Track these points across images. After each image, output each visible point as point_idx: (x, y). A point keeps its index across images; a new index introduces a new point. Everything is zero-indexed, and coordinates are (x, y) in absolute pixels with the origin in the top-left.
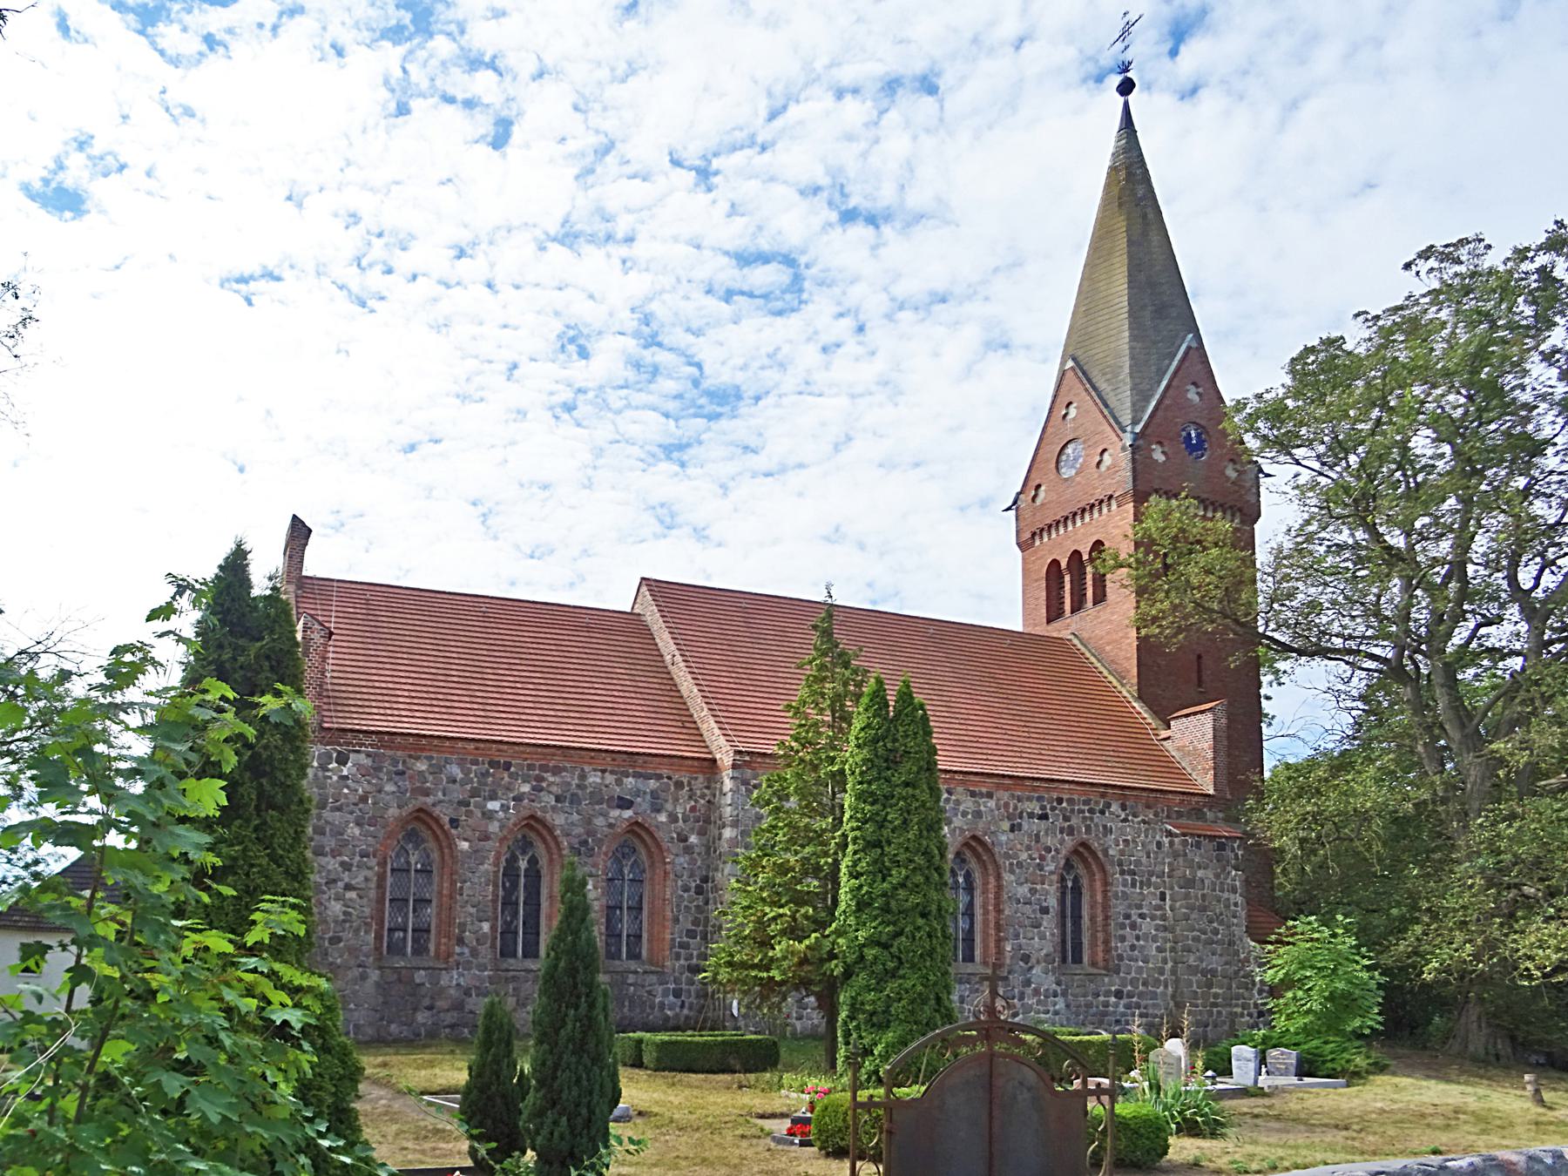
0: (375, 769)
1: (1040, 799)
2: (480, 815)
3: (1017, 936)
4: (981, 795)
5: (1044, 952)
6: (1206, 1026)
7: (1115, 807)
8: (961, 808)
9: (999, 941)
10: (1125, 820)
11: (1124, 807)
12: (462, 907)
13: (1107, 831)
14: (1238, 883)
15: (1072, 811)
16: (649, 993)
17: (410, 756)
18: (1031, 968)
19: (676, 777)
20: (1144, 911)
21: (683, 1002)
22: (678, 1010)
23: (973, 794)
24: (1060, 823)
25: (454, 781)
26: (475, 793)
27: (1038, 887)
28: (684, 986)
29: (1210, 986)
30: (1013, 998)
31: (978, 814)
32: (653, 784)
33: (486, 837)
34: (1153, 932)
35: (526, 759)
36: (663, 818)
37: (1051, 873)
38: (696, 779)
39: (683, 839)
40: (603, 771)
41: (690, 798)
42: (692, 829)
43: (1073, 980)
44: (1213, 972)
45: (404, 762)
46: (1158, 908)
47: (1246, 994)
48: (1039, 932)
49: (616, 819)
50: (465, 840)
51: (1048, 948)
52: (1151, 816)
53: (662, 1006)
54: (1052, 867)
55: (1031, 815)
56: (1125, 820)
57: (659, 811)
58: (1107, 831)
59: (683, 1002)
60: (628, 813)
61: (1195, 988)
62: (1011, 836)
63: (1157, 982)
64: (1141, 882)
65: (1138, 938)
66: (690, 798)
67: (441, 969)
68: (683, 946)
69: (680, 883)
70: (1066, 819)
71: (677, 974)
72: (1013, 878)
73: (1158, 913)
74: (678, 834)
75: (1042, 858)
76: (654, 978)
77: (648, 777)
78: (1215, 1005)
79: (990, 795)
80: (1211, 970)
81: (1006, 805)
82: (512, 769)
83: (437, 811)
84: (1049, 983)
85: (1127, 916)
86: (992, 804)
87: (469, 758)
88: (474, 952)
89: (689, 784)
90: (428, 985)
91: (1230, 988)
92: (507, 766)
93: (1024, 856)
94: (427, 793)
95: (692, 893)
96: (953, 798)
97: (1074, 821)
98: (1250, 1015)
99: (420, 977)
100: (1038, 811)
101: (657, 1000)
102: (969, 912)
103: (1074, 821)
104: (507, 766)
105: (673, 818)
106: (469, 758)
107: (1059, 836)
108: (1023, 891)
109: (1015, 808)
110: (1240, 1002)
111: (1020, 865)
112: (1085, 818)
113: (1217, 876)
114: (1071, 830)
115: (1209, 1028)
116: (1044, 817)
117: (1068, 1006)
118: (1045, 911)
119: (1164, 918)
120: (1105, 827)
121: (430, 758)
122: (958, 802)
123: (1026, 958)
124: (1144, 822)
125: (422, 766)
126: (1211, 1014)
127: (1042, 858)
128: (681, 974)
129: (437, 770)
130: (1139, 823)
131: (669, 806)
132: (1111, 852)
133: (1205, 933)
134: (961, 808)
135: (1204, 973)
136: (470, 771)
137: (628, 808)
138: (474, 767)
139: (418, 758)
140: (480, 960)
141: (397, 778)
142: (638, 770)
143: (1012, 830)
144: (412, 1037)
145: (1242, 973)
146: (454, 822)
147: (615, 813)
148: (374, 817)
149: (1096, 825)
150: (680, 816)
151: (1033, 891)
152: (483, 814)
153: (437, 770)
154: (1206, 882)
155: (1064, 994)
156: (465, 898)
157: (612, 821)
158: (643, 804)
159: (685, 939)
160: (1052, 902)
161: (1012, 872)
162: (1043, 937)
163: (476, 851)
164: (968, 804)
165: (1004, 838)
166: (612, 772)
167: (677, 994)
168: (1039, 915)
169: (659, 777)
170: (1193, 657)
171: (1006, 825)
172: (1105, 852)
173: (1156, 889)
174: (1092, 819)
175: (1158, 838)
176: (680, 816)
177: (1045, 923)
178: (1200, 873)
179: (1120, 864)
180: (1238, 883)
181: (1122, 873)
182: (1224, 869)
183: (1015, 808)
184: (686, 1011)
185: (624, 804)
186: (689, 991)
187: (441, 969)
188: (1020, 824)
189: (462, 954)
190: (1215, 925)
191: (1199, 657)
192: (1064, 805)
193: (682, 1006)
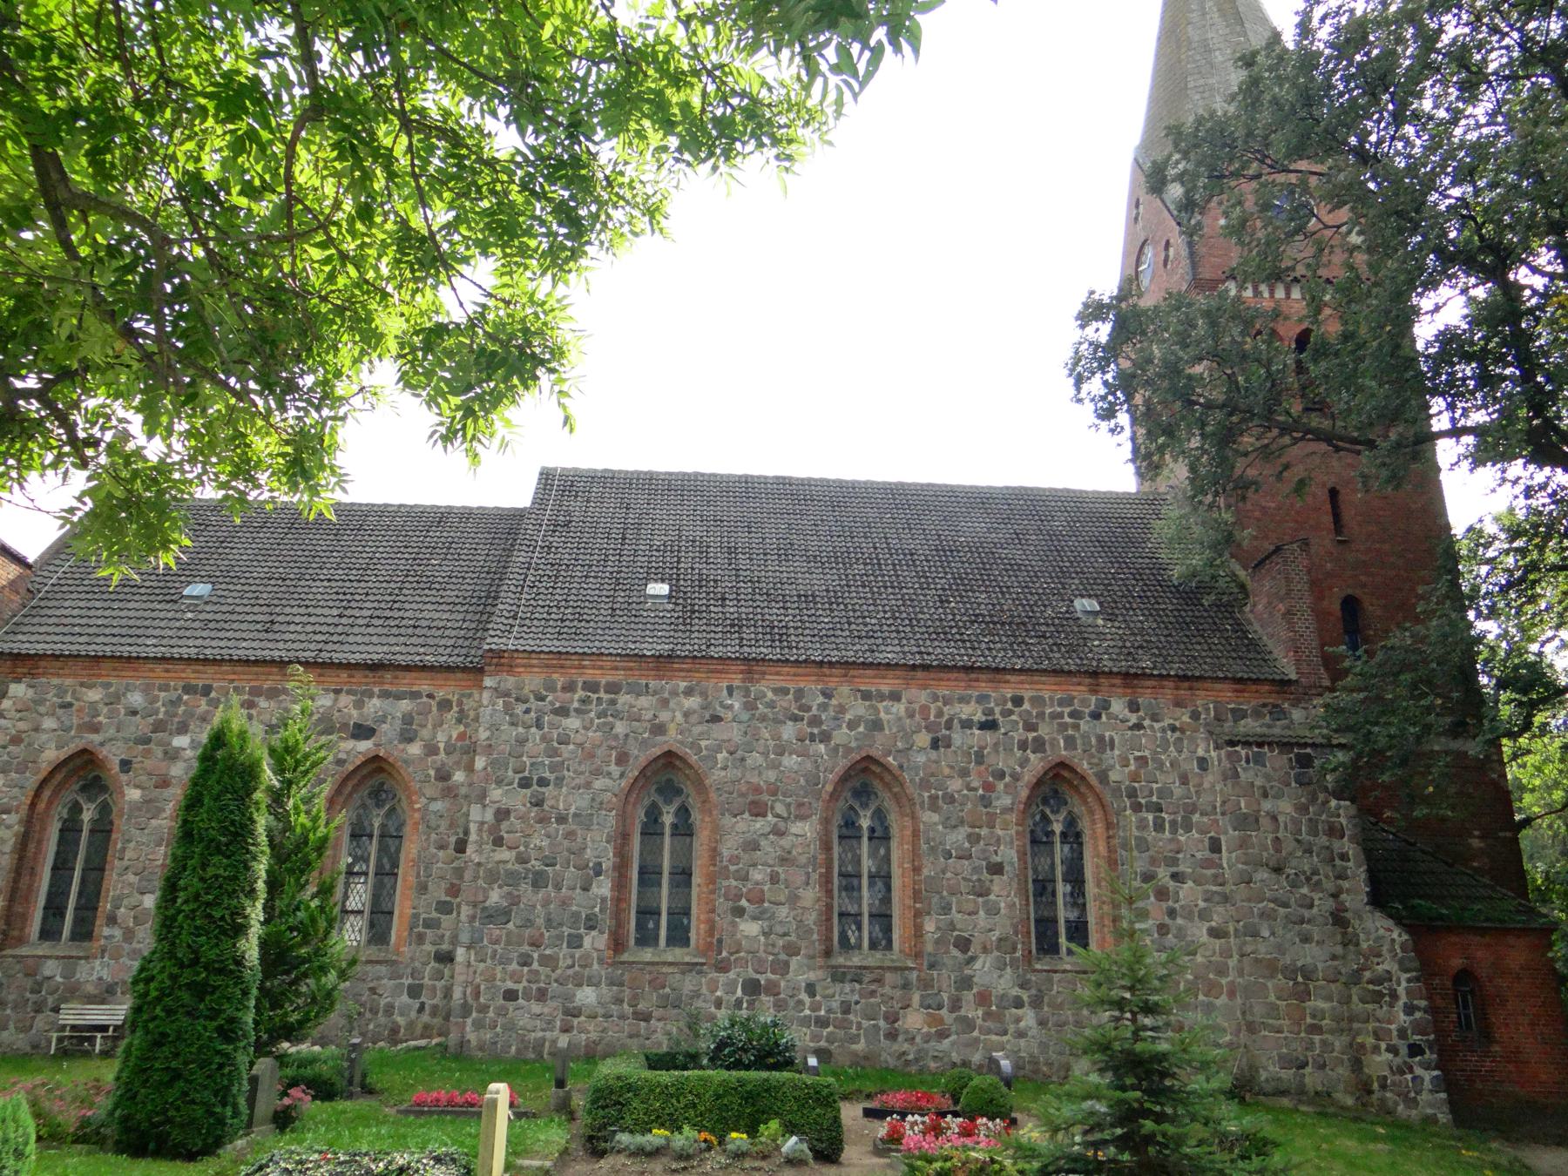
0: (34, 702)
1: (982, 699)
2: (160, 755)
3: (946, 909)
4: (882, 697)
5: (997, 933)
6: (1303, 1065)
7: (1118, 706)
8: (848, 717)
9: (918, 914)
10: (1139, 726)
11: (1134, 707)
12: (120, 875)
13: (1104, 744)
14: (1343, 821)
15: (1041, 715)
16: (373, 990)
17: (82, 685)
18: (973, 959)
19: (440, 694)
20: (1181, 868)
21: (423, 1005)
22: (413, 1014)
23: (866, 696)
24: (1019, 734)
25: (134, 713)
26: (159, 727)
27: (984, 832)
28: (426, 981)
29: (1304, 995)
30: (940, 1007)
31: (877, 725)
32: (405, 705)
33: (164, 783)
34: (1202, 904)
35: (232, 681)
36: (415, 749)
37: (1006, 810)
38: (470, 695)
39: (443, 776)
40: (337, 692)
41: (459, 721)
42: (457, 763)
43: (1050, 981)
44: (1308, 973)
45: (74, 692)
46: (1207, 863)
47: (1380, 1013)
48: (985, 903)
49: (348, 753)
50: (137, 787)
51: (1002, 926)
52: (1186, 719)
53: (389, 1010)
54: (1007, 801)
55: (967, 724)
56: (1139, 726)
57: (410, 740)
58: (1104, 744)
59: (423, 1005)
60: (365, 746)
61: (1272, 998)
62: (933, 755)
63: (1212, 990)
64: (1173, 823)
65: (1172, 913)
66: (459, 721)
67: (80, 958)
68: (428, 924)
69: (433, 836)
70: (1030, 727)
71: (417, 964)
72: (936, 817)
73: (1209, 872)
74: (438, 770)
75: (989, 787)
76: (383, 969)
77: (399, 697)
78: (1315, 1029)
79: (895, 697)
80: (1303, 969)
81: (925, 709)
82: (213, 694)
83: (103, 752)
84: (1005, 984)
85: (1148, 877)
86: (900, 708)
87: (157, 682)
88: (129, 935)
89: (460, 703)
90: (59, 979)
91: (1347, 1000)
92: (207, 690)
93: (955, 785)
94: (96, 729)
95: (451, 851)
96: (834, 702)
97: (1044, 731)
98: (1393, 1050)
99: (51, 968)
100: (979, 717)
101: (383, 1002)
102: (882, 877)
103: (1044, 731)
104: (207, 690)
105: (431, 750)
106: (157, 682)
107: (1019, 754)
108: (958, 837)
109: (940, 714)
110: (1371, 1026)
111: (951, 799)
112: (1064, 727)
113: (1303, 809)
114: (1039, 745)
115: (1308, 1070)
116: (989, 725)
117: (1042, 1023)
118: (997, 869)
119: (1219, 880)
120: (1101, 739)
121: (107, 686)
122: (842, 709)
123: (964, 944)
124: (1173, 729)
125: (94, 695)
126: (1310, 1046)
127: (989, 787)
128: (425, 964)
129: (113, 700)
130: (1163, 730)
131: (425, 733)
132: (1114, 776)
133: (1285, 905)
134: (848, 717)
135: (1290, 972)
136: (155, 699)
137: (367, 738)
138: (163, 694)
139: (90, 687)
140: (135, 945)
141: (60, 712)
142: (386, 687)
143: (935, 744)
144: (28, 1049)
145: (1367, 974)
146: (126, 765)
147: (349, 744)
148: (25, 762)
149: (1085, 737)
150: (442, 746)
151: (974, 839)
152: (166, 753)
153: (113, 700)
154: (1281, 819)
155: (1036, 1003)
156: (126, 863)
157: (342, 756)
158: (388, 730)
159: (435, 915)
160: (1008, 854)
161: (934, 807)
162: (993, 911)
163: (150, 801)
164: (859, 708)
165: (921, 759)
166: (349, 692)
167: (414, 992)
168: (985, 876)
169: (415, 695)
170: (1323, 495)
171: (923, 739)
172: (1103, 777)
173: (1201, 832)
174: (1076, 727)
175: (1200, 752)
176: (442, 746)
177: (996, 888)
178: (1267, 805)
179: (1132, 794)
180: (1343, 821)
181: (1137, 808)
182: (1314, 799)
183: (940, 714)
184: (425, 1018)
185: (362, 731)
186: (434, 988)
187: (80, 958)
188: (949, 738)
189: (112, 937)
190: (1305, 890)
191: (1334, 493)
192: (1026, 706)
193: (421, 1009)
